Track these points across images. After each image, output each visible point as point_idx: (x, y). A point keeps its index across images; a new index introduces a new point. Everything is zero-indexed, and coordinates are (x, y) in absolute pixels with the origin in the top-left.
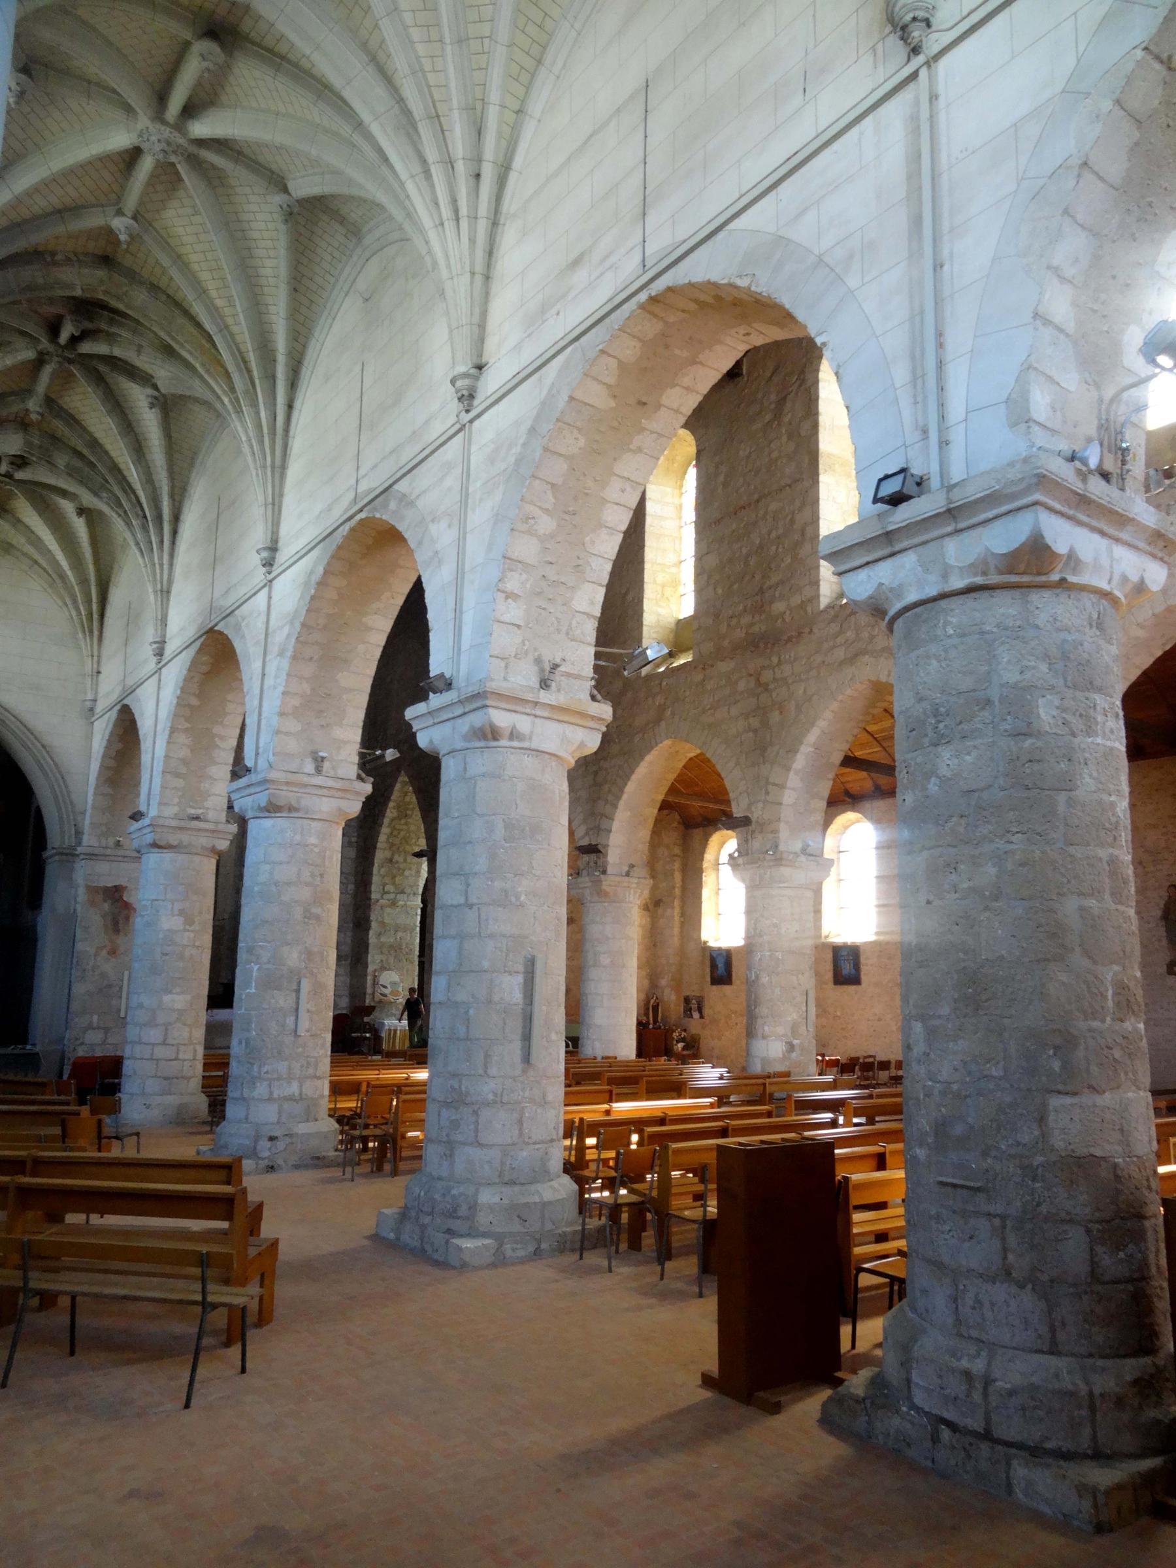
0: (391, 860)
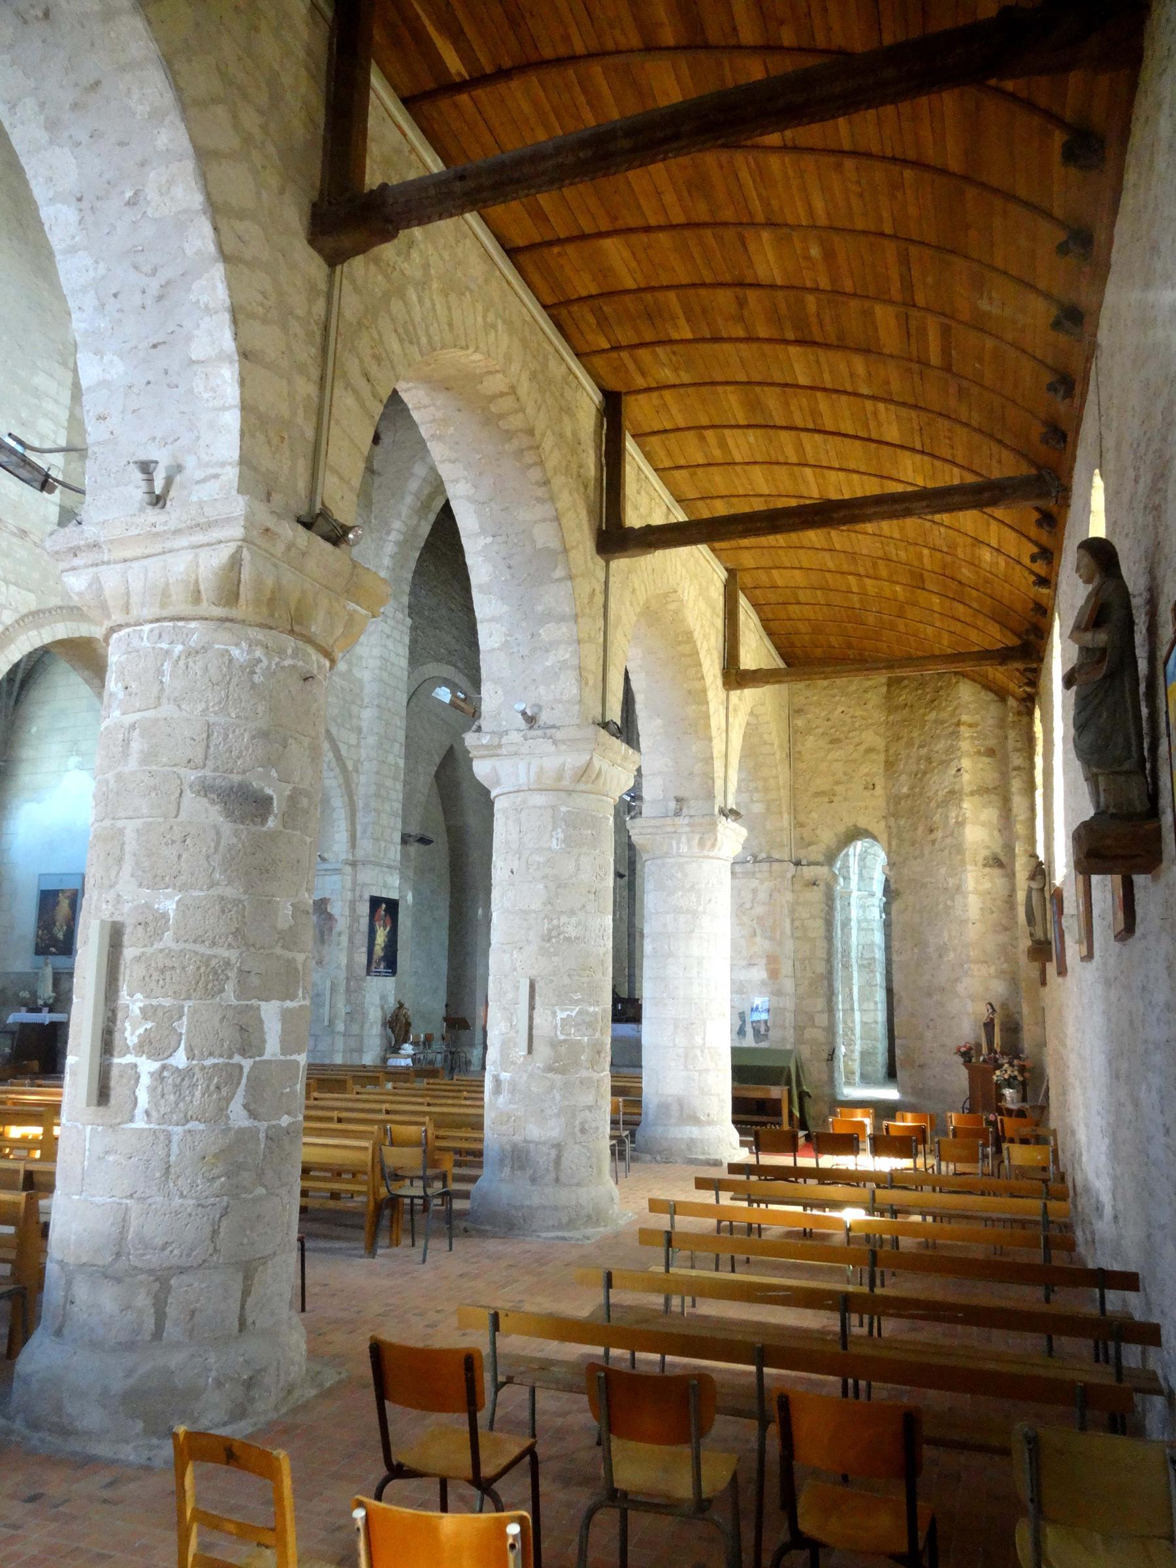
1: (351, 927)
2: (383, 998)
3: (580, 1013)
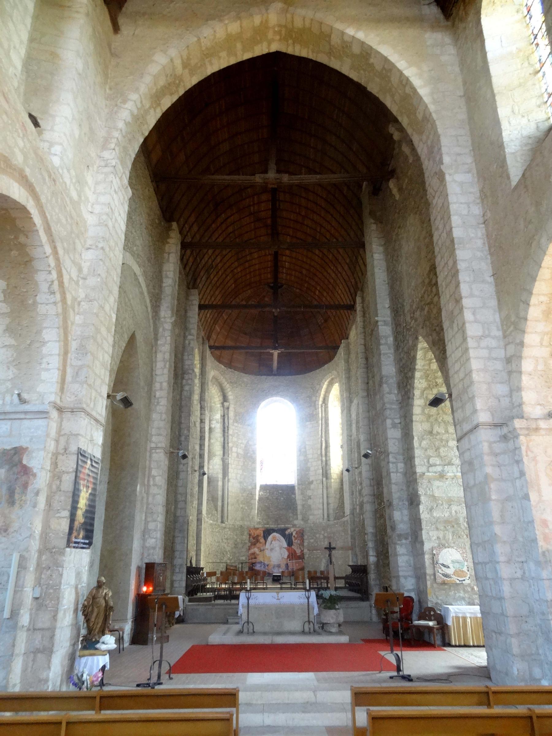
0: (431, 433)
1: (50, 486)
2: (78, 575)
3: (257, 585)
